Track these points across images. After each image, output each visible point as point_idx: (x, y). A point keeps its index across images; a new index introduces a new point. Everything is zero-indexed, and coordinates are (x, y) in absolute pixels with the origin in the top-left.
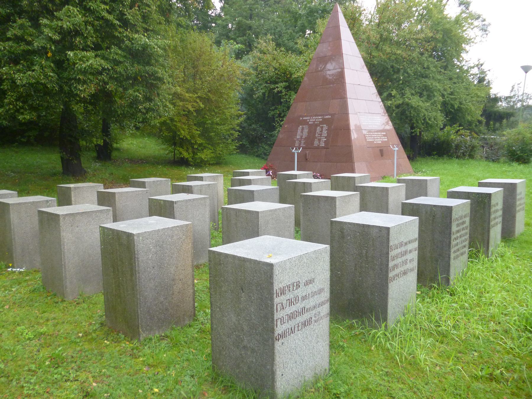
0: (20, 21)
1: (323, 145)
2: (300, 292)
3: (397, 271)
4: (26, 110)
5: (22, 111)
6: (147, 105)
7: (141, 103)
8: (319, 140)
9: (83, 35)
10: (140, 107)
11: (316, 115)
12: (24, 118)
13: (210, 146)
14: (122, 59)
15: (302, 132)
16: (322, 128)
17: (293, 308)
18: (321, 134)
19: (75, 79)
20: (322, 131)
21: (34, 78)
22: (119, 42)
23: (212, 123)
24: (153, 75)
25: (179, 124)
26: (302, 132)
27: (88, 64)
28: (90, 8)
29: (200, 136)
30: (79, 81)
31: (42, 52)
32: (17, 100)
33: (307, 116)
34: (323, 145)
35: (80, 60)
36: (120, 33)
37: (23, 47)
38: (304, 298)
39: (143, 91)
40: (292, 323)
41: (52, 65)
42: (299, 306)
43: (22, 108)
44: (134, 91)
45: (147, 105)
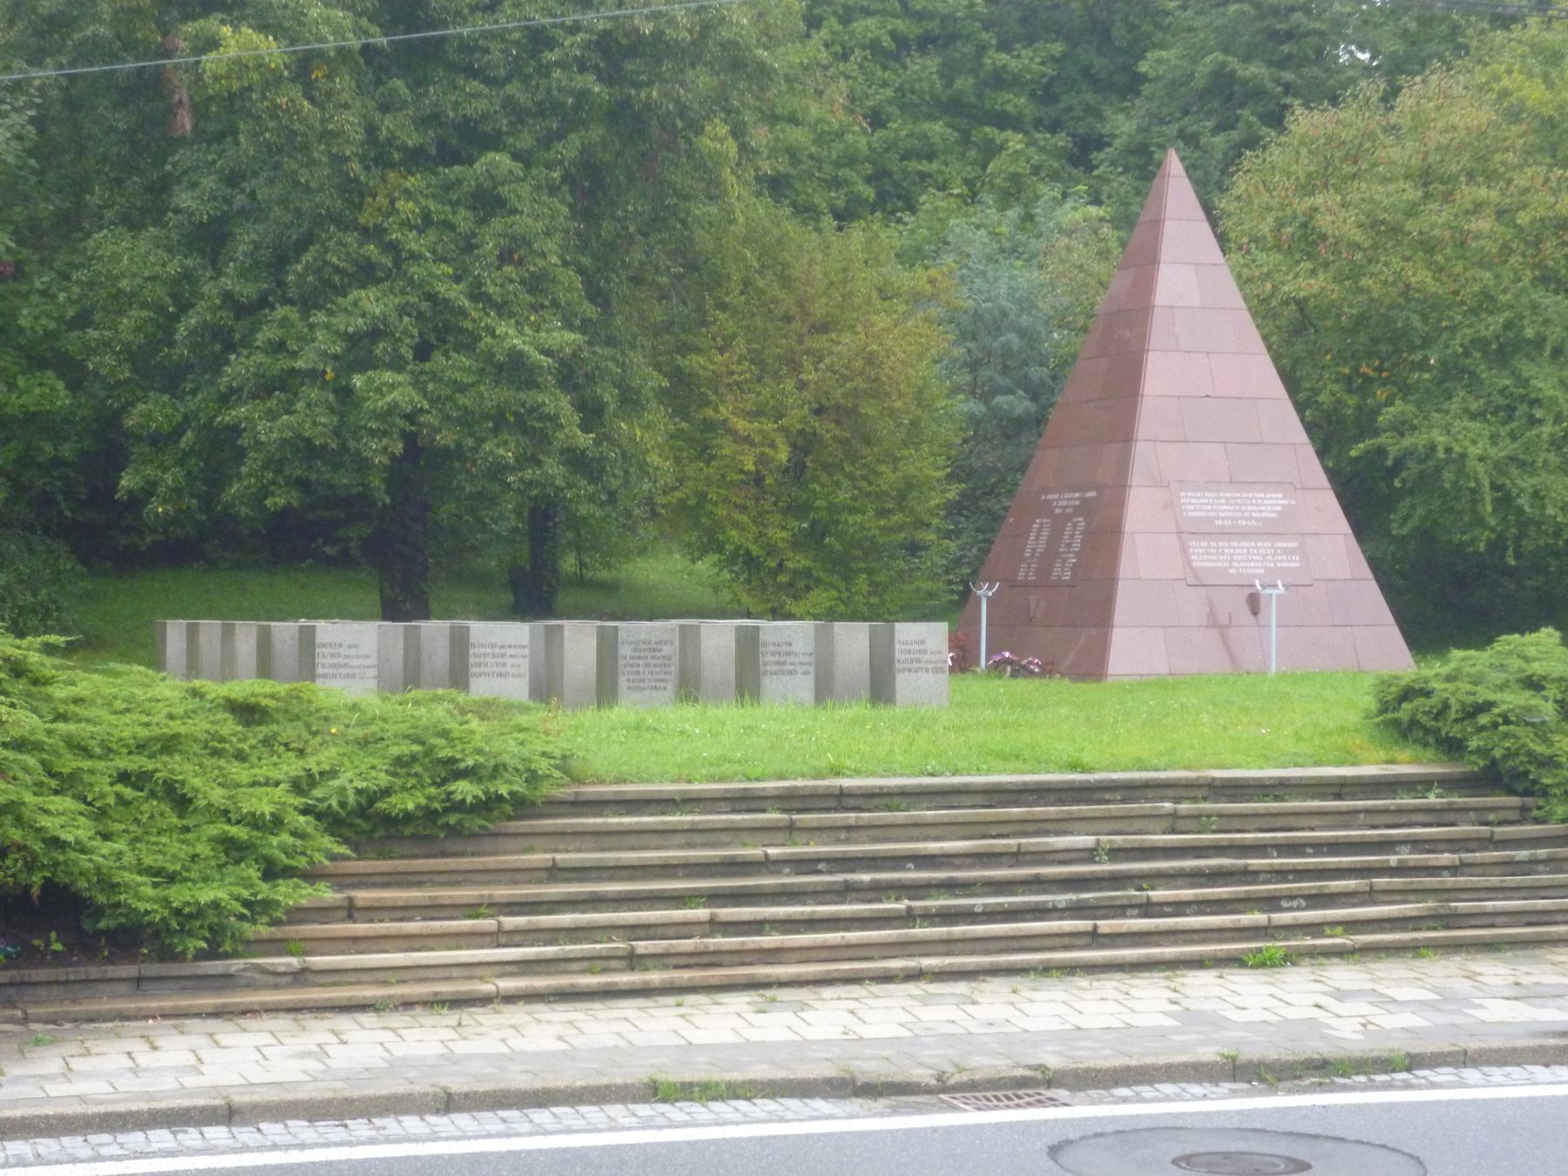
0: (281, 311)
1: (1067, 576)
2: (342, 651)
3: (482, 669)
4: (280, 487)
5: (272, 488)
6: (528, 474)
7: (513, 470)
8: (1064, 561)
9: (393, 334)
10: (510, 479)
11: (1072, 489)
12: (275, 504)
13: (835, 579)
14: (468, 379)
15: (1037, 538)
16: (1075, 525)
17: (335, 661)
18: (1069, 545)
19: (365, 427)
20: (1072, 537)
21: (291, 428)
22: (468, 344)
23: (832, 508)
24: (533, 410)
25: (721, 512)
26: (1037, 538)
27: (389, 398)
28: (412, 278)
29: (795, 545)
30: (372, 433)
31: (313, 375)
32: (265, 467)
33: (1053, 492)
34: (1067, 576)
35: (378, 390)
36: (474, 321)
37: (284, 363)
38: (347, 657)
39: (518, 445)
40: (332, 671)
41: (331, 397)
42: (342, 660)
43: (272, 482)
44: (498, 445)
45: (528, 474)
